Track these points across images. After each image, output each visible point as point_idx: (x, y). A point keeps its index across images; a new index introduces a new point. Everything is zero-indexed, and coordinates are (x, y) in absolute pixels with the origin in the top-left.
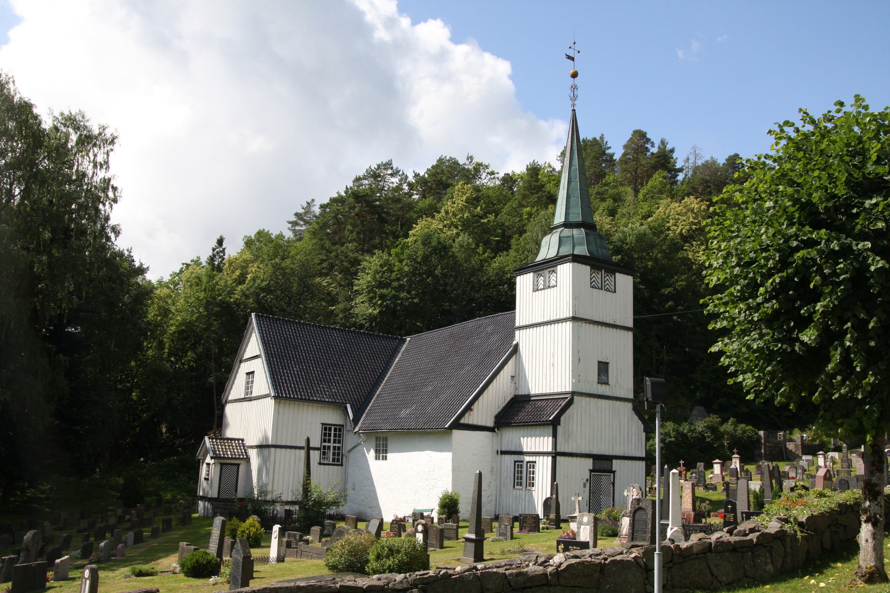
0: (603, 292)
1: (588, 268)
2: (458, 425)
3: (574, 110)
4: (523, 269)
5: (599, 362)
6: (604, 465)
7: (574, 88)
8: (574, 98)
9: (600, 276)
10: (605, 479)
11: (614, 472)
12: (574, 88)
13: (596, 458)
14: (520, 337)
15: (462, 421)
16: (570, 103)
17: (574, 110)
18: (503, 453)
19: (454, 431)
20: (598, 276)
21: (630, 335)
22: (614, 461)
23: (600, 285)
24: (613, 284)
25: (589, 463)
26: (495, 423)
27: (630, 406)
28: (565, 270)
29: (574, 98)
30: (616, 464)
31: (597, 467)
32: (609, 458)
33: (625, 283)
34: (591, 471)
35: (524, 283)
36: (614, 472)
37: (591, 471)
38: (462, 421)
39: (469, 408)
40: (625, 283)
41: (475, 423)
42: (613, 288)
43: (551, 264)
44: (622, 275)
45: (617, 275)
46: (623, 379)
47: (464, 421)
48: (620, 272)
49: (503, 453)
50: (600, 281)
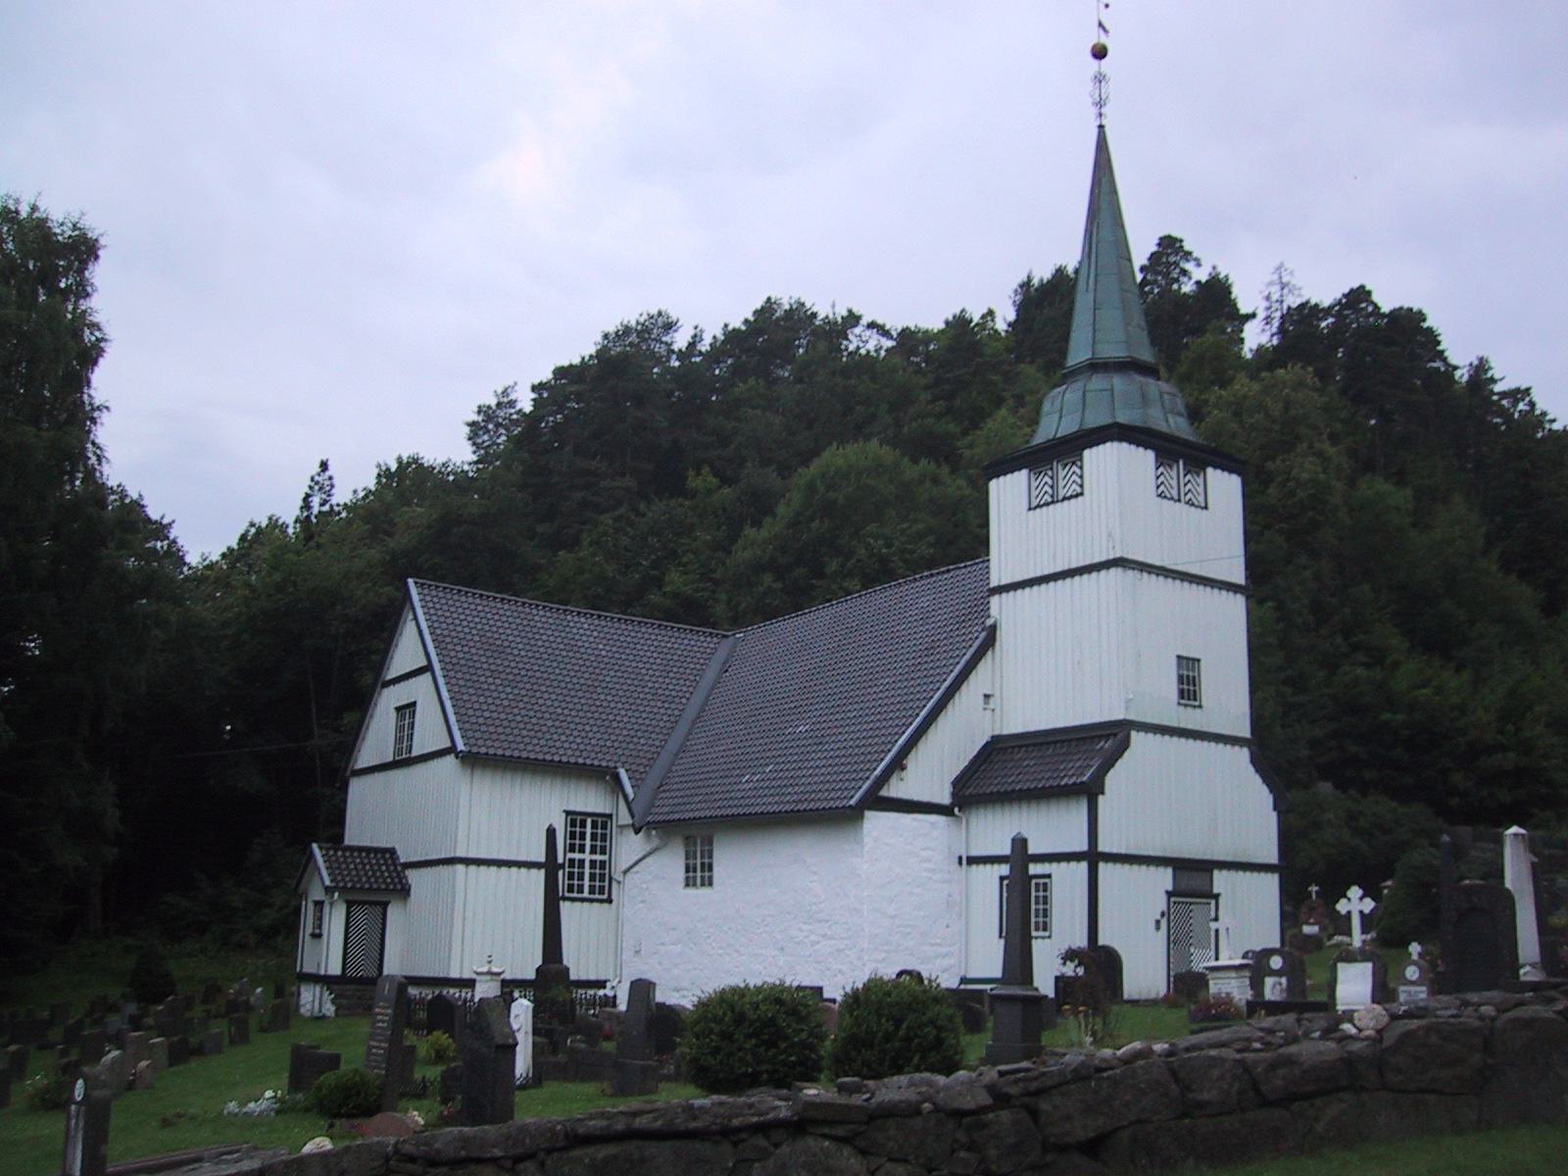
0: (1181, 507)
1: (1150, 455)
2: (877, 801)
3: (1101, 127)
4: (1004, 466)
5: (1179, 657)
6: (1194, 881)
7: (1100, 79)
8: (1100, 104)
9: (1174, 473)
10: (1198, 910)
11: (1216, 897)
12: (1100, 79)
13: (1181, 866)
14: (1000, 608)
15: (884, 793)
16: (1094, 111)
17: (1101, 127)
18: (973, 861)
19: (868, 814)
20: (1173, 475)
21: (1237, 605)
22: (1216, 873)
23: (1174, 493)
24: (1201, 489)
25: (1164, 878)
26: (954, 795)
27: (1243, 754)
28: (1102, 460)
29: (1100, 104)
30: (1221, 880)
31: (1183, 886)
32: (1207, 867)
33: (1225, 488)
34: (1169, 894)
35: (1008, 493)
36: (1216, 897)
37: (1169, 894)
38: (884, 793)
39: (898, 764)
40: (1225, 488)
41: (916, 797)
42: (1201, 499)
43: (1070, 448)
44: (1219, 472)
45: (1210, 471)
46: (1229, 699)
47: (895, 789)
48: (1215, 467)
49: (973, 861)
50: (1174, 483)
